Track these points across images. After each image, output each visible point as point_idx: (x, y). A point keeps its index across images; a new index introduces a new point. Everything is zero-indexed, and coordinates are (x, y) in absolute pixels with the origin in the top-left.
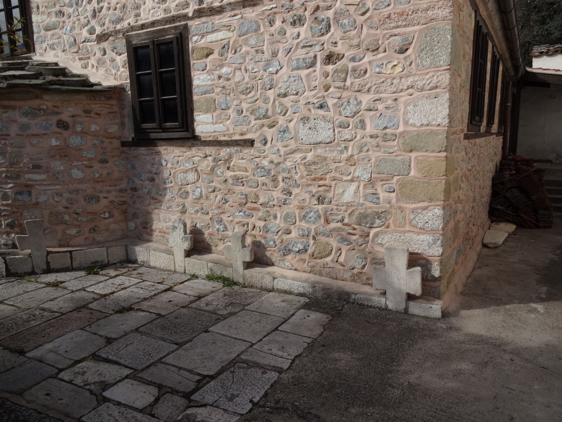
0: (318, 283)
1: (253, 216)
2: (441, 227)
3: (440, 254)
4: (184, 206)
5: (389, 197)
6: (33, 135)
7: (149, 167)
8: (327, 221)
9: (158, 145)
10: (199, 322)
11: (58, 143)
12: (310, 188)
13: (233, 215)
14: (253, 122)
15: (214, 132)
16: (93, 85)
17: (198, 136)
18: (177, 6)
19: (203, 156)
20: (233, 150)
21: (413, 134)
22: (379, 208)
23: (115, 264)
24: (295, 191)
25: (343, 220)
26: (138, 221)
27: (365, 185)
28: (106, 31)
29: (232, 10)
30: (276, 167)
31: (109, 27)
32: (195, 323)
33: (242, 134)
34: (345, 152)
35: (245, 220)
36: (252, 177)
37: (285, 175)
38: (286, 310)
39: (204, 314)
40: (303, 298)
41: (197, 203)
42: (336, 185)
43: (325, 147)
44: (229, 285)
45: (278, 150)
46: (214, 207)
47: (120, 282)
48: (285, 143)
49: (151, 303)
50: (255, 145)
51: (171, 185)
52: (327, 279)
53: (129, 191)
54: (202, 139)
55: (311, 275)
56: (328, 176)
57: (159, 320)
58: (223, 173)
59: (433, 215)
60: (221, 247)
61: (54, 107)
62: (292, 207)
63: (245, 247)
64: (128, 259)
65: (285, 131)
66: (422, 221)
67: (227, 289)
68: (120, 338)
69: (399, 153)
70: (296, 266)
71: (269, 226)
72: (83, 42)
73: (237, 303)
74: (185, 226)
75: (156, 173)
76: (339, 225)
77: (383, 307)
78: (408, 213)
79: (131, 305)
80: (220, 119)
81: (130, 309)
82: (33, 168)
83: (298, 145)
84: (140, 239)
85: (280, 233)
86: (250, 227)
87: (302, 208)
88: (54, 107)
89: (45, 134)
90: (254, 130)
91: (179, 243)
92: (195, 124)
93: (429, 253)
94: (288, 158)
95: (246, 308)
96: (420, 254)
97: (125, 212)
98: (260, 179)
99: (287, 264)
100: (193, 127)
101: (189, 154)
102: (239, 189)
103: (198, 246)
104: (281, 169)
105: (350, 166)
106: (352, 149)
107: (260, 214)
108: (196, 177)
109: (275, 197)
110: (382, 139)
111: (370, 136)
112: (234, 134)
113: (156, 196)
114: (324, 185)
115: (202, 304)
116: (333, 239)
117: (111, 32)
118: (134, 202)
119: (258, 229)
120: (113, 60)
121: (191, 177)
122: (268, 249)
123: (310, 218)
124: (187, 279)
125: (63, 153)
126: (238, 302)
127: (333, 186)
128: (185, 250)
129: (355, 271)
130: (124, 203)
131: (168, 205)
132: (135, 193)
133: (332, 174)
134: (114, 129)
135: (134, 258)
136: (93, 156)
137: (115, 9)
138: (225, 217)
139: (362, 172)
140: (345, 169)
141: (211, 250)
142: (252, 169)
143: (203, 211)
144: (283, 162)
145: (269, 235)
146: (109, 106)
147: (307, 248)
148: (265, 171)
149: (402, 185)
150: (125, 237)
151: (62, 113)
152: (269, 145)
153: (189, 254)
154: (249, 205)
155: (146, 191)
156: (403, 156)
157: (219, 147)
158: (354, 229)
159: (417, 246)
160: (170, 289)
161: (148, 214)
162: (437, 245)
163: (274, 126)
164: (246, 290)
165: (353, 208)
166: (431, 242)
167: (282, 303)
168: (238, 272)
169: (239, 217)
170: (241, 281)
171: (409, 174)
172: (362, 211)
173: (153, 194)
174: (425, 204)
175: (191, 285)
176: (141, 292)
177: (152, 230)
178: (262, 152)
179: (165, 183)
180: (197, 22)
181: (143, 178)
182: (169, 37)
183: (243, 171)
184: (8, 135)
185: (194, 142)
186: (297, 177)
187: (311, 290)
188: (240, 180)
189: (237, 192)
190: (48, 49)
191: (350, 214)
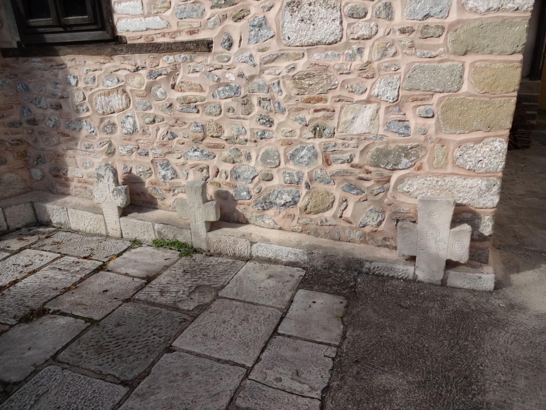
0: (316, 247)
1: (215, 157)
2: (501, 167)
3: (495, 205)
4: (111, 145)
5: (424, 125)
7: (50, 87)
8: (327, 162)
9: (60, 52)
10: (155, 330)
12: (302, 115)
13: (184, 155)
14: (209, 12)
15: (147, 29)
17: (121, 37)
19: (133, 68)
20: (179, 57)
21: (472, 25)
22: (408, 141)
23: (18, 229)
24: (278, 119)
25: (352, 160)
26: (46, 167)
27: (387, 108)
30: (248, 83)
32: (149, 333)
33: (192, 32)
34: (358, 57)
35: (204, 163)
36: (211, 100)
37: (263, 95)
38: (278, 294)
39: (160, 313)
40: (295, 269)
41: (130, 140)
42: (342, 108)
43: (326, 50)
44: (187, 254)
45: (251, 56)
46: (155, 145)
47: (26, 261)
48: (261, 45)
49: (75, 297)
50: (214, 50)
51: (88, 114)
52: (326, 240)
53: (25, 125)
54: (129, 42)
55: (303, 235)
56: (330, 96)
57: (90, 333)
58: (165, 94)
59: (491, 150)
60: (170, 200)
62: (274, 142)
63: (208, 201)
64: (37, 220)
65: (260, 26)
66: (473, 159)
67: (185, 261)
68: (26, 380)
69: (445, 57)
70: (280, 224)
71: (240, 170)
73: (205, 286)
74: (115, 173)
75: (62, 97)
76: (346, 166)
77: (411, 277)
78: (451, 148)
79: (45, 303)
80: (154, 8)
81: (41, 312)
83: (283, 47)
84: (51, 191)
85: (257, 179)
86: (212, 172)
87: (290, 144)
90: (210, 25)
91: (110, 198)
92: (115, 17)
93: (479, 203)
94: (267, 68)
95: (220, 294)
96: (465, 205)
97: (24, 155)
98: (223, 102)
99: (267, 222)
100: (113, 23)
101: (109, 65)
102: (192, 117)
103: (137, 199)
104: (255, 86)
105: (365, 80)
106: (370, 52)
107: (226, 153)
108: (124, 101)
109: (247, 128)
110: (419, 35)
111: (400, 30)
112: (179, 32)
113: (67, 131)
114: (324, 109)
115: (152, 291)
116: (335, 186)
118: (36, 141)
119: (224, 175)
121: (117, 101)
122: (239, 202)
123: (302, 157)
124: (125, 247)
126: (207, 283)
127: (337, 110)
128: (119, 207)
129: (367, 229)
130: (20, 142)
131: (86, 143)
132: (35, 127)
133: (337, 92)
135: (46, 219)
138: (173, 159)
139: (383, 88)
140: (357, 84)
141: (156, 204)
142: (211, 87)
143: (139, 151)
144: (259, 76)
145: (240, 183)
147: (296, 199)
148: (231, 89)
149: (447, 107)
150: (29, 189)
152: (235, 48)
153: (124, 212)
154: (208, 140)
155: (51, 124)
156: (452, 61)
157: (156, 55)
158: (368, 172)
159: (461, 195)
160: (102, 268)
161: (59, 156)
162: (492, 192)
163: (243, 17)
164: (214, 260)
165: (367, 143)
166: (484, 189)
167: (269, 281)
168: (199, 236)
169: (195, 158)
170: (204, 246)
171: (459, 89)
172: (381, 146)
173: (62, 128)
174: (480, 135)
175: (134, 257)
176: (60, 277)
177: (67, 179)
178: (226, 59)
179: (78, 111)
181: (43, 104)
183: (196, 90)
185: (116, 47)
186: (280, 98)
187: (306, 257)
188: (193, 105)
189: (189, 122)
191: (362, 152)
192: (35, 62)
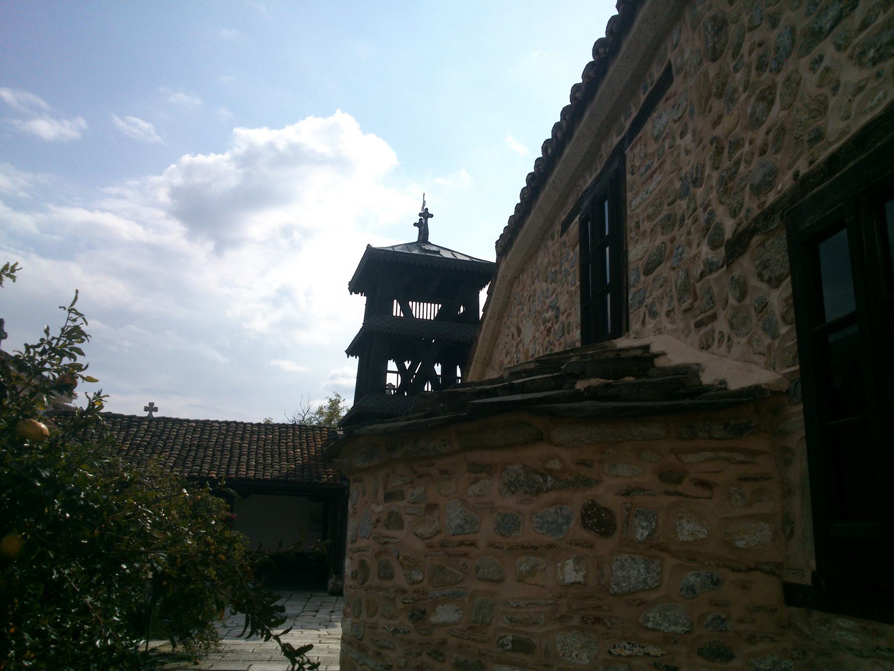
6: (523, 547)
11: (580, 578)
16: (702, 390)
28: (745, 223)
31: (752, 206)
61: (582, 463)
72: (702, 275)
82: (513, 650)
88: (582, 463)
89: (550, 546)
117: (756, 220)
120: (763, 307)
125: (589, 610)
134: (754, 537)
136: (679, 629)
137: (763, 152)
146: (740, 457)
151: (599, 482)
184: (472, 544)
190: (648, 319)
192: (841, 628)
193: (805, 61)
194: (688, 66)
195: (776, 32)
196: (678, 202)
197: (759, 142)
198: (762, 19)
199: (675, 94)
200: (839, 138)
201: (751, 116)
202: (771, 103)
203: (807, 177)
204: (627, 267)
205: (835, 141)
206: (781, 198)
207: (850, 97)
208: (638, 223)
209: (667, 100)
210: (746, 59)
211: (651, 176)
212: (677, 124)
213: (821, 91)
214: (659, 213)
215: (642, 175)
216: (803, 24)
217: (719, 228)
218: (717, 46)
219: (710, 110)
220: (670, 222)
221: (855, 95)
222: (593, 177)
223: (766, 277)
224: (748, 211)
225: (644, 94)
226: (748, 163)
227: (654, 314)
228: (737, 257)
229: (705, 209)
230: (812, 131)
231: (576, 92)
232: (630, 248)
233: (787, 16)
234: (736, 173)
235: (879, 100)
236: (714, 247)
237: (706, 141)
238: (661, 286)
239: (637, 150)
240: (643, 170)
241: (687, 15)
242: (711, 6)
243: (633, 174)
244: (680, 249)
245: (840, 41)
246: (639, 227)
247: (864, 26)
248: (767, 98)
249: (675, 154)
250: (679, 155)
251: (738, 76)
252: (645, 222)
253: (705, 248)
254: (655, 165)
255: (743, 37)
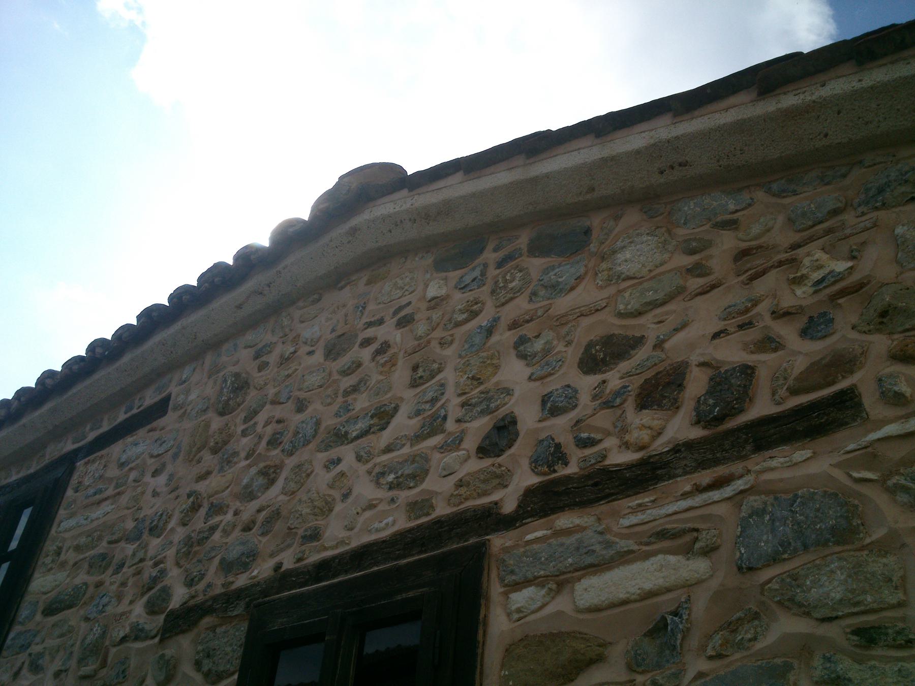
18: (460, 484)
28: (201, 598)
29: (702, 465)
31: (215, 581)
72: (124, 639)
117: (215, 599)
137: (247, 528)
180: (536, 531)
182: (411, 594)
190: (24, 671)
193: (322, 457)
194: (190, 408)
195: (299, 417)
196: (122, 544)
197: (245, 516)
198: (289, 398)
199: (163, 429)
200: (336, 547)
201: (247, 486)
202: (272, 482)
203: (290, 573)
204: (22, 597)
205: (332, 548)
206: (253, 586)
207: (359, 510)
208: (60, 548)
209: (150, 431)
210: (259, 429)
211: (99, 503)
212: (153, 460)
213: (332, 492)
214: (93, 548)
215: (87, 497)
216: (329, 422)
217: (166, 593)
218: (231, 402)
219: (199, 462)
220: (101, 562)
221: (364, 510)
222: (22, 474)
223: (205, 669)
224: (209, 585)
225: (126, 413)
226: (226, 533)
227: (36, 668)
228: (177, 634)
229: (156, 564)
230: (310, 528)
231: (48, 377)
232: (37, 575)
233: (316, 407)
234: (207, 538)
235: (387, 524)
236: (152, 609)
237: (183, 491)
238: (62, 636)
239: (92, 468)
240: (91, 491)
241: (209, 359)
242: (238, 361)
243: (76, 491)
244: (105, 600)
245: (362, 453)
246: (59, 554)
247: (388, 449)
248: (269, 475)
249: (139, 490)
250: (143, 493)
251: (245, 440)
252: (71, 550)
253: (138, 610)
254: (110, 492)
255: (263, 406)
